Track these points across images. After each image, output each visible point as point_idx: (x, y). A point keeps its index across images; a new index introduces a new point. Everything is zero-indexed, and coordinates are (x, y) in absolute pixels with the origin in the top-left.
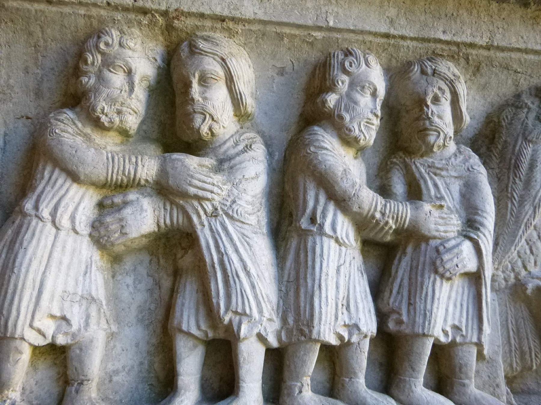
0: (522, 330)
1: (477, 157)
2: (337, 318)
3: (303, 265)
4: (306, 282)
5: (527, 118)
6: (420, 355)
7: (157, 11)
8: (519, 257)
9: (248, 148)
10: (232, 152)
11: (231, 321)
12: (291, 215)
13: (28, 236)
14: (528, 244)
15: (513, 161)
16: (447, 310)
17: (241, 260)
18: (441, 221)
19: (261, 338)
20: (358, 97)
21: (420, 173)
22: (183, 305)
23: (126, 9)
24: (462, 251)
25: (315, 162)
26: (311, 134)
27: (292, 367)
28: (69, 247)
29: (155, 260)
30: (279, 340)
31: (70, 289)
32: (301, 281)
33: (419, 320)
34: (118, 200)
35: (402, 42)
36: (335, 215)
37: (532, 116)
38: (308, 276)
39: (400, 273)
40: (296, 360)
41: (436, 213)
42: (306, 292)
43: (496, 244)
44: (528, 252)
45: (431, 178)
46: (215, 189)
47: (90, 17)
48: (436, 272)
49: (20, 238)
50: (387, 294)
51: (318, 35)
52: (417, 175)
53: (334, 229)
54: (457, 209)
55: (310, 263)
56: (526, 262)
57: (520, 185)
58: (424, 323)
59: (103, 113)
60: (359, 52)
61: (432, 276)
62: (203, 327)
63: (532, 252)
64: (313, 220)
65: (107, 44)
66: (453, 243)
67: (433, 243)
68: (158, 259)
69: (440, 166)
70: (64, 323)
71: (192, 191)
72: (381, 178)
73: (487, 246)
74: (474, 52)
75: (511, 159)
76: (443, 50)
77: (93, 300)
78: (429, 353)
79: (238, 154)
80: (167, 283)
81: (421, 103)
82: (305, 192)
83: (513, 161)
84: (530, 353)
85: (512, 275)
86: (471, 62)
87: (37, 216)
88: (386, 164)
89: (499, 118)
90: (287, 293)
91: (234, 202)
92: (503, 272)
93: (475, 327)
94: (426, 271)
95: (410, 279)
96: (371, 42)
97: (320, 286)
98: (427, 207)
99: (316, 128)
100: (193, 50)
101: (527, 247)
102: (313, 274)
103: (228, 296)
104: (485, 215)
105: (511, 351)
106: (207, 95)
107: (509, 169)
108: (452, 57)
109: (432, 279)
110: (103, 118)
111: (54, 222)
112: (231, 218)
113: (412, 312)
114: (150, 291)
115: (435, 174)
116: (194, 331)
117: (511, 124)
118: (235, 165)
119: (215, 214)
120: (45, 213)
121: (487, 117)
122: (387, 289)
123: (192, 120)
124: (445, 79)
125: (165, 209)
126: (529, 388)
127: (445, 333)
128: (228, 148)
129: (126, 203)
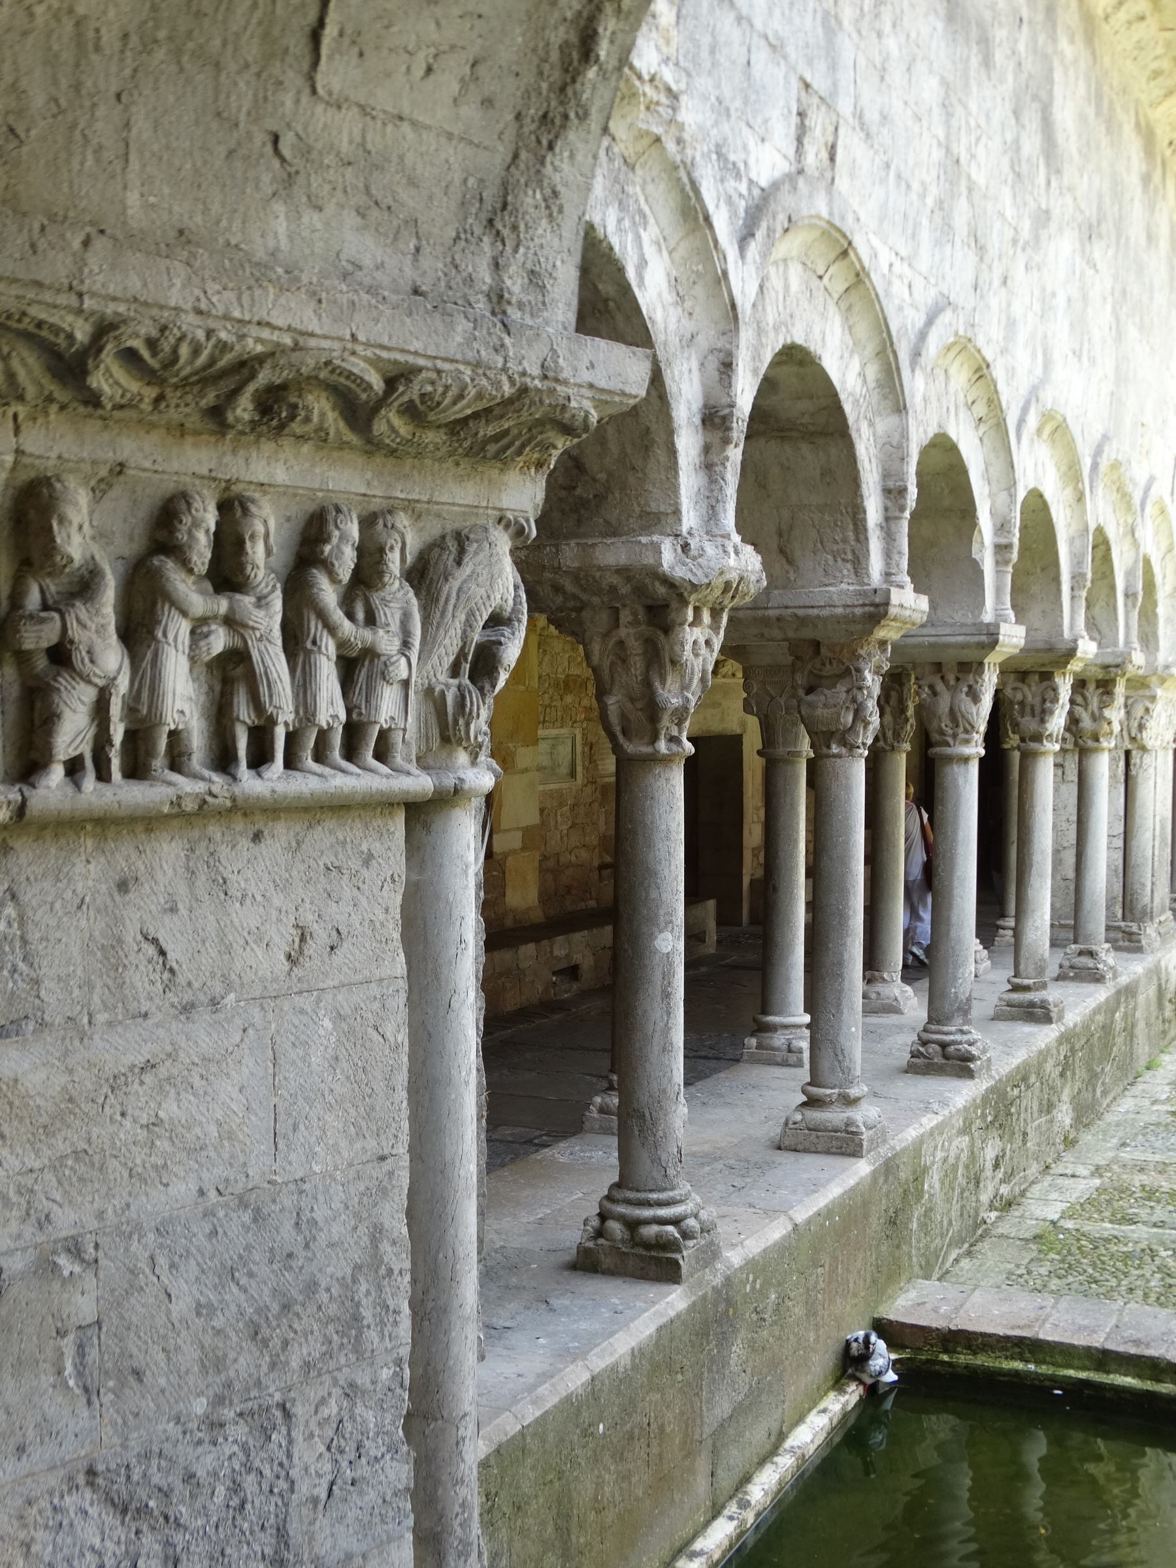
9: (274, 587)
10: (265, 591)
12: (295, 637)
23: (203, 477)
37: (452, 558)
57: (438, 614)
64: (314, 643)
67: (383, 659)
71: (251, 623)
73: (414, 661)
81: (381, 550)
98: (381, 632)
103: (271, 696)
108: (404, 509)
119: (260, 640)
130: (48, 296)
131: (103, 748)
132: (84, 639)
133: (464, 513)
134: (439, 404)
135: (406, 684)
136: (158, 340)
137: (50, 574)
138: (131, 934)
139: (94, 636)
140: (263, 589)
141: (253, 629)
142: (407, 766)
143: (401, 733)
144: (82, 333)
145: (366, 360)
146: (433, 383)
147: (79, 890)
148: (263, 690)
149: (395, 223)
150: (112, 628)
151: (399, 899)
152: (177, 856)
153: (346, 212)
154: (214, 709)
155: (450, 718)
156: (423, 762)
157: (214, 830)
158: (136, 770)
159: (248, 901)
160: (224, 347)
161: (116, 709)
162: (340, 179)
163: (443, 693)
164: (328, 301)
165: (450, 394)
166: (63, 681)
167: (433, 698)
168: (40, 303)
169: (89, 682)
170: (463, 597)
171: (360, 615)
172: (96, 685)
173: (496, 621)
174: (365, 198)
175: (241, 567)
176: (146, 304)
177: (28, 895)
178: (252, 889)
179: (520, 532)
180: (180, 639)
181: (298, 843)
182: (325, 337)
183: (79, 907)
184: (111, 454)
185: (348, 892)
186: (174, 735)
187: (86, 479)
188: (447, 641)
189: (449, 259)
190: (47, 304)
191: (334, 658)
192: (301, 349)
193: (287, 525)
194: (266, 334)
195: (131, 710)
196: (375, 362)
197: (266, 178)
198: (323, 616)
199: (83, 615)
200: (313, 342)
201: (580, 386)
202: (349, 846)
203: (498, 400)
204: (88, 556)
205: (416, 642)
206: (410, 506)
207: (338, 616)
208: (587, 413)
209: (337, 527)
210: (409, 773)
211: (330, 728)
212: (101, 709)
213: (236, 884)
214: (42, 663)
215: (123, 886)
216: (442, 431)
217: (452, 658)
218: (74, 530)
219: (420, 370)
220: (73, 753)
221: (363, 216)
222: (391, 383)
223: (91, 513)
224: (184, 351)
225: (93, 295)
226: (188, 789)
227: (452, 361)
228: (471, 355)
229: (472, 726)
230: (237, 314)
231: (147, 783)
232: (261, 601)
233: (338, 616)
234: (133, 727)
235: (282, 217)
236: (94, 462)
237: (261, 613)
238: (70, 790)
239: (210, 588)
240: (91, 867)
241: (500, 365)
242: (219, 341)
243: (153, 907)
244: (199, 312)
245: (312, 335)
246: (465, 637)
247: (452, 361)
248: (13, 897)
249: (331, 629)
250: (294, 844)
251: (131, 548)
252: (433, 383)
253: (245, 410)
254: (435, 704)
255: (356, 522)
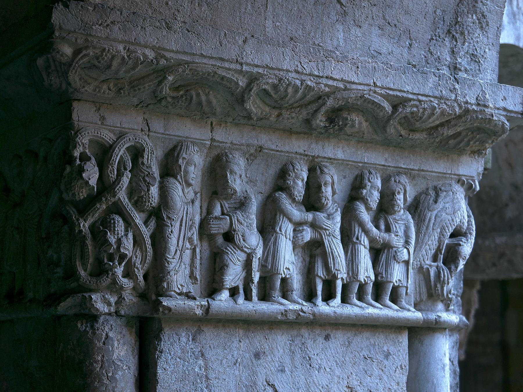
0: (421, 285)
1: (410, 216)
2: (364, 274)
3: (354, 255)
4: (356, 260)
5: (430, 200)
6: (388, 288)
7: (310, 155)
8: (422, 256)
9: (337, 210)
10: (332, 212)
11: (335, 272)
12: (348, 236)
13: (280, 240)
14: (425, 251)
15: (423, 218)
16: (397, 274)
17: (338, 252)
18: (397, 241)
19: (342, 279)
20: (373, 191)
21: (391, 221)
22: (318, 267)
23: (301, 154)
24: (404, 252)
25: (359, 217)
26: (357, 206)
27: (351, 290)
28: (289, 245)
29: (303, 251)
30: (347, 281)
31: (289, 259)
32: (354, 260)
33: (389, 276)
34: (301, 228)
35: (389, 168)
36: (364, 237)
37: (432, 199)
38: (356, 258)
39: (382, 260)
40: (352, 287)
41: (396, 238)
42: (356, 264)
43: (415, 251)
44: (425, 254)
45: (394, 224)
46: (331, 227)
47: (289, 156)
48: (395, 260)
49: (277, 241)
50: (378, 267)
51: (361, 165)
52: (390, 222)
53: (364, 243)
54: (402, 237)
55: (357, 254)
56: (424, 258)
58: (391, 277)
59: (296, 196)
60: (374, 172)
61: (394, 261)
62: (325, 275)
63: (426, 254)
64: (357, 239)
65: (297, 170)
66: (401, 249)
67: (395, 249)
68: (305, 251)
69: (398, 219)
70: (288, 270)
72: (376, 222)
73: (412, 251)
74: (413, 172)
75: (422, 217)
76: (402, 171)
77: (293, 263)
78: (391, 288)
79: (334, 213)
80: (308, 259)
81: (393, 194)
82: (355, 228)
83: (423, 218)
84: (423, 294)
85: (419, 263)
86: (412, 176)
87: (281, 233)
88: (378, 216)
89: (419, 198)
90: (349, 265)
91: (335, 231)
92: (416, 262)
93: (406, 281)
94: (392, 259)
95: (386, 262)
96: (378, 168)
97: (360, 262)
99: (358, 203)
100: (322, 171)
101: (425, 252)
102: (358, 258)
103: (334, 264)
104: (412, 239)
105: (416, 293)
106: (327, 190)
107: (421, 221)
108: (406, 174)
109: (393, 262)
110: (297, 199)
111: (286, 236)
112: (334, 237)
113: (387, 274)
114: (302, 262)
115: (396, 222)
116: (322, 276)
117: (423, 202)
118: (334, 217)
119: (329, 235)
120: (283, 233)
121: (415, 197)
122: (378, 266)
123: (322, 199)
124: (402, 185)
125: (313, 232)
126: (421, 309)
127: (396, 281)
128: (331, 210)
129: (303, 230)
130: (227, 65)
131: (249, 284)
132: (240, 229)
133: (438, 177)
134: (421, 118)
135: (407, 263)
136: (278, 85)
137: (225, 199)
138: (261, 381)
139: (245, 229)
140: (331, 210)
141: (326, 229)
142: (408, 307)
143: (405, 289)
144: (242, 83)
145: (381, 95)
146: (417, 107)
147: (235, 355)
148: (331, 260)
149: (399, 32)
150: (255, 225)
151: (405, 379)
152: (285, 343)
153: (373, 28)
154: (306, 270)
155: (432, 283)
156: (417, 306)
157: (305, 332)
158: (265, 297)
159: (322, 371)
160: (309, 88)
161: (255, 264)
162: (370, 12)
163: (428, 269)
164: (362, 67)
165: (426, 113)
166: (230, 249)
167: (423, 272)
168: (222, 68)
169: (242, 251)
170: (438, 220)
171: (383, 227)
172: (245, 252)
173: (457, 234)
174: (383, 21)
175: (319, 199)
176: (272, 68)
177: (210, 354)
178: (324, 364)
179: (470, 188)
180: (288, 233)
181: (349, 342)
182: (360, 84)
183: (235, 364)
184: (256, 142)
185: (376, 372)
186: (284, 280)
187: (244, 154)
188: (430, 242)
189: (428, 49)
190: (226, 69)
191: (368, 247)
192: (348, 90)
193: (344, 180)
194: (330, 82)
195: (263, 267)
196: (386, 97)
197: (333, 13)
198: (362, 225)
199: (241, 218)
200: (354, 87)
201: (498, 109)
202: (377, 347)
203: (453, 116)
204: (244, 190)
205: (413, 241)
206: (408, 172)
207: (370, 226)
208: (503, 123)
209: (369, 181)
210: (409, 310)
211: (366, 283)
212: (248, 265)
213: (316, 361)
214: (220, 240)
215: (257, 356)
216: (424, 133)
217: (433, 252)
218: (237, 177)
219: (410, 100)
220: (234, 285)
221: (382, 30)
222: (395, 107)
223: (246, 170)
224: (290, 90)
225: (248, 64)
226: (291, 307)
227: (427, 96)
228: (437, 93)
229: (445, 288)
230: (316, 73)
231: (269, 303)
232: (329, 217)
233: (370, 226)
234: (264, 275)
235: (341, 30)
236: (248, 145)
237: (330, 222)
238: (231, 303)
239: (304, 209)
240: (241, 344)
241: (453, 98)
242: (307, 86)
243: (272, 368)
244: (297, 72)
245: (354, 83)
246: (440, 241)
247: (427, 96)
248: (203, 355)
249: (366, 232)
250: (347, 343)
251: (266, 189)
252: (417, 107)
253: (321, 121)
254: (424, 275)
255: (379, 179)
